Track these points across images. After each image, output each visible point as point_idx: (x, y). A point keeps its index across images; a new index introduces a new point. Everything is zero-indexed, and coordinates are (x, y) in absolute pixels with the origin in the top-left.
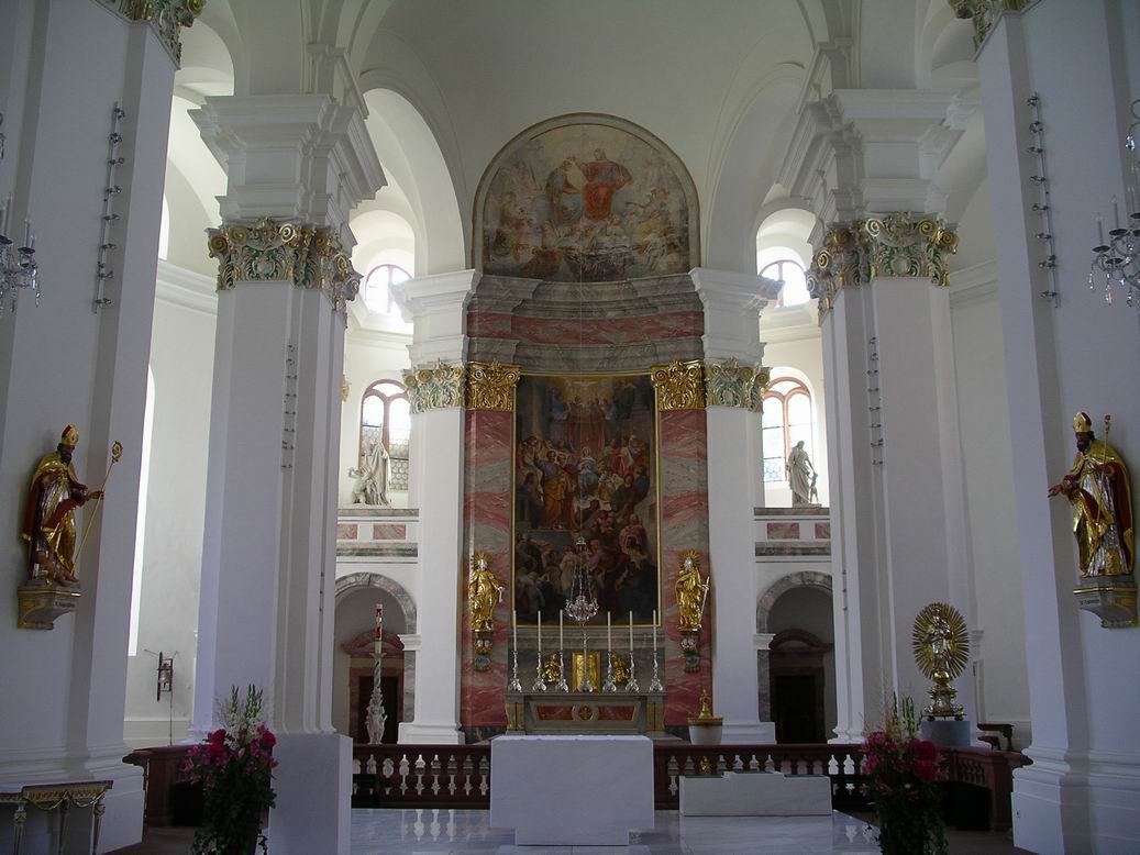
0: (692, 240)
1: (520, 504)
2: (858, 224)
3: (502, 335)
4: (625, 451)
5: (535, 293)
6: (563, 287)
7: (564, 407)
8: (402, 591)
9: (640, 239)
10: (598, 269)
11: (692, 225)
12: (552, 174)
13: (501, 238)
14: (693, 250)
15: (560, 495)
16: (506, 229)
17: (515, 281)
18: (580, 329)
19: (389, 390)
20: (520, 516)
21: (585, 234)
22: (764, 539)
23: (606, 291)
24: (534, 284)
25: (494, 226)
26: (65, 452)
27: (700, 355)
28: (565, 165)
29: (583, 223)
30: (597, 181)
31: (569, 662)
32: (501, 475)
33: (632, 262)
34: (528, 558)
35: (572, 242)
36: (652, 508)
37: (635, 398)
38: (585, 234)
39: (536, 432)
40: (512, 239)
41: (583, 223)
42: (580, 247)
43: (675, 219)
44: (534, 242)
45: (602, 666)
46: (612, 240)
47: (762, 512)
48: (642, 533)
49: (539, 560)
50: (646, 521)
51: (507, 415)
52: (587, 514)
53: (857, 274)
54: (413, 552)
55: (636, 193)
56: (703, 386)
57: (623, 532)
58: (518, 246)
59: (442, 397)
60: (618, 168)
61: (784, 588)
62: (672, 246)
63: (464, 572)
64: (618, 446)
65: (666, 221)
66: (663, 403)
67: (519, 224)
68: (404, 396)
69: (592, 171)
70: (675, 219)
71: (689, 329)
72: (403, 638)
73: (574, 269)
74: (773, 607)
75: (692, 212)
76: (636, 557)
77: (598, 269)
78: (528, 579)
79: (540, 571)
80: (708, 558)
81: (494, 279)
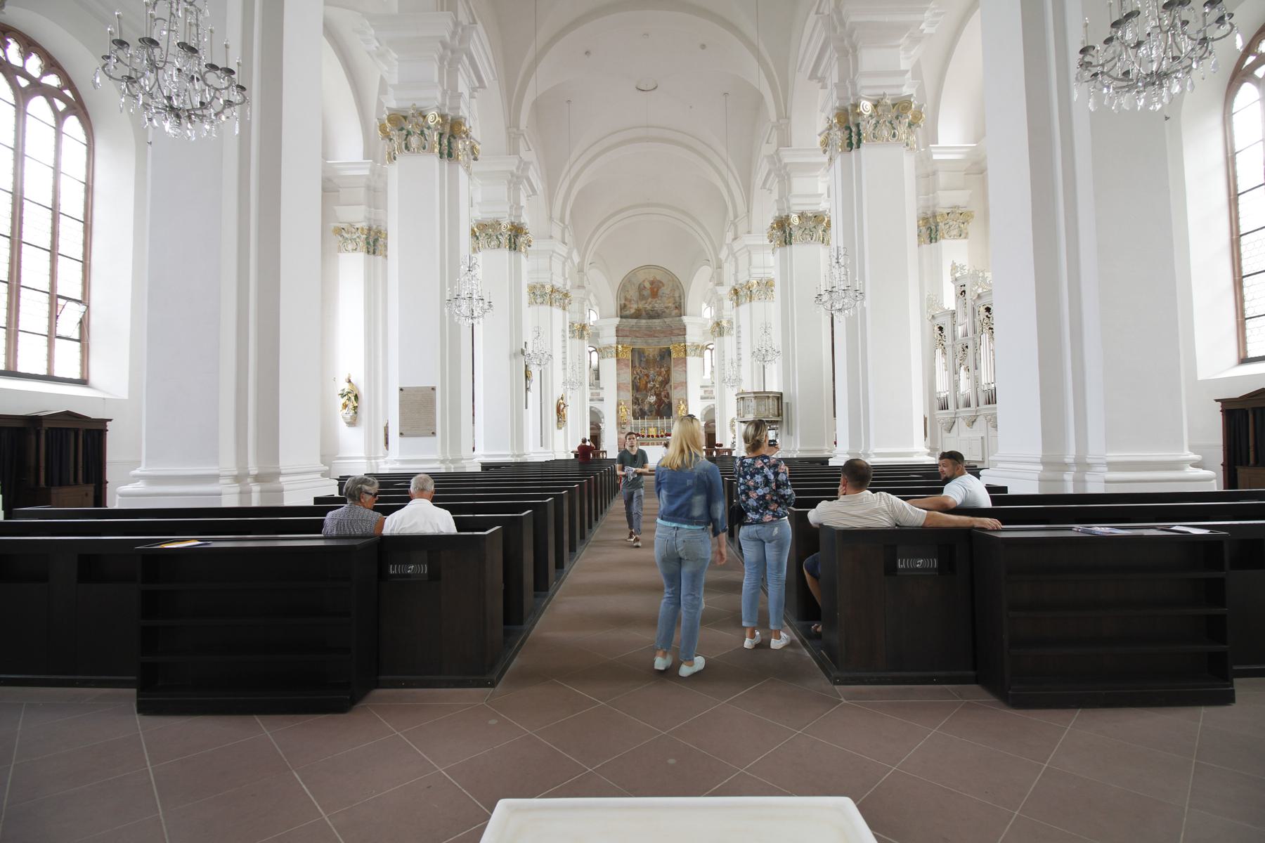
0: (682, 304)
1: (633, 386)
2: (721, 322)
3: (627, 336)
4: (663, 369)
5: (636, 323)
6: (644, 321)
7: (645, 357)
8: (600, 411)
9: (666, 305)
10: (653, 315)
11: (682, 300)
12: (640, 285)
13: (625, 306)
14: (682, 309)
15: (644, 382)
16: (627, 303)
17: (630, 320)
18: (648, 333)
19: (591, 349)
20: (633, 389)
21: (650, 303)
22: (703, 394)
23: (657, 321)
24: (635, 320)
25: (623, 302)
26: (562, 399)
27: (685, 342)
28: (644, 281)
29: (650, 300)
30: (653, 286)
31: (648, 430)
32: (627, 377)
33: (664, 312)
34: (636, 401)
35: (646, 306)
36: (671, 386)
37: (665, 354)
38: (650, 303)
39: (637, 365)
40: (629, 306)
41: (650, 300)
42: (649, 307)
43: (677, 299)
44: (635, 306)
45: (658, 431)
46: (658, 305)
47: (702, 387)
48: (668, 394)
49: (638, 401)
50: (669, 391)
51: (628, 360)
52: (652, 388)
53: (721, 334)
54: (602, 400)
55: (665, 290)
56: (686, 351)
57: (663, 393)
58: (630, 308)
59: (609, 355)
60: (661, 282)
61: (709, 408)
62: (676, 307)
63: (618, 406)
64: (661, 368)
65: (675, 300)
66: (674, 355)
67: (630, 301)
68: (596, 350)
69: (652, 283)
70: (677, 299)
71: (681, 333)
72: (600, 425)
73: (647, 314)
74: (706, 414)
75: (682, 297)
76: (666, 400)
77: (653, 315)
78: (635, 407)
79: (639, 405)
80: (687, 401)
81: (624, 320)
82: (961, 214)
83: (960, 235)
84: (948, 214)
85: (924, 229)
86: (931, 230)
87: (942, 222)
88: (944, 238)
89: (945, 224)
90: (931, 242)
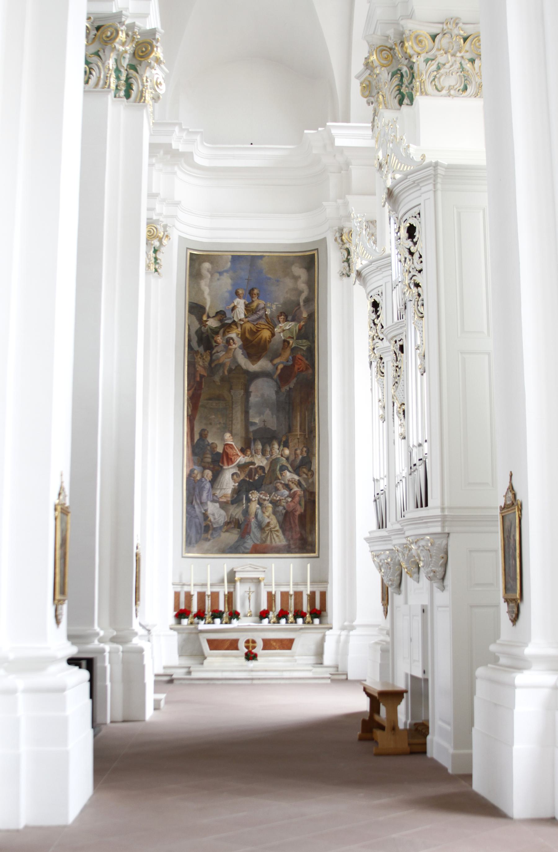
82: (465, 39)
83: (465, 89)
84: (434, 37)
85: (384, 75)
86: (402, 76)
87: (419, 54)
88: (424, 93)
89: (427, 61)
90: (401, 103)
